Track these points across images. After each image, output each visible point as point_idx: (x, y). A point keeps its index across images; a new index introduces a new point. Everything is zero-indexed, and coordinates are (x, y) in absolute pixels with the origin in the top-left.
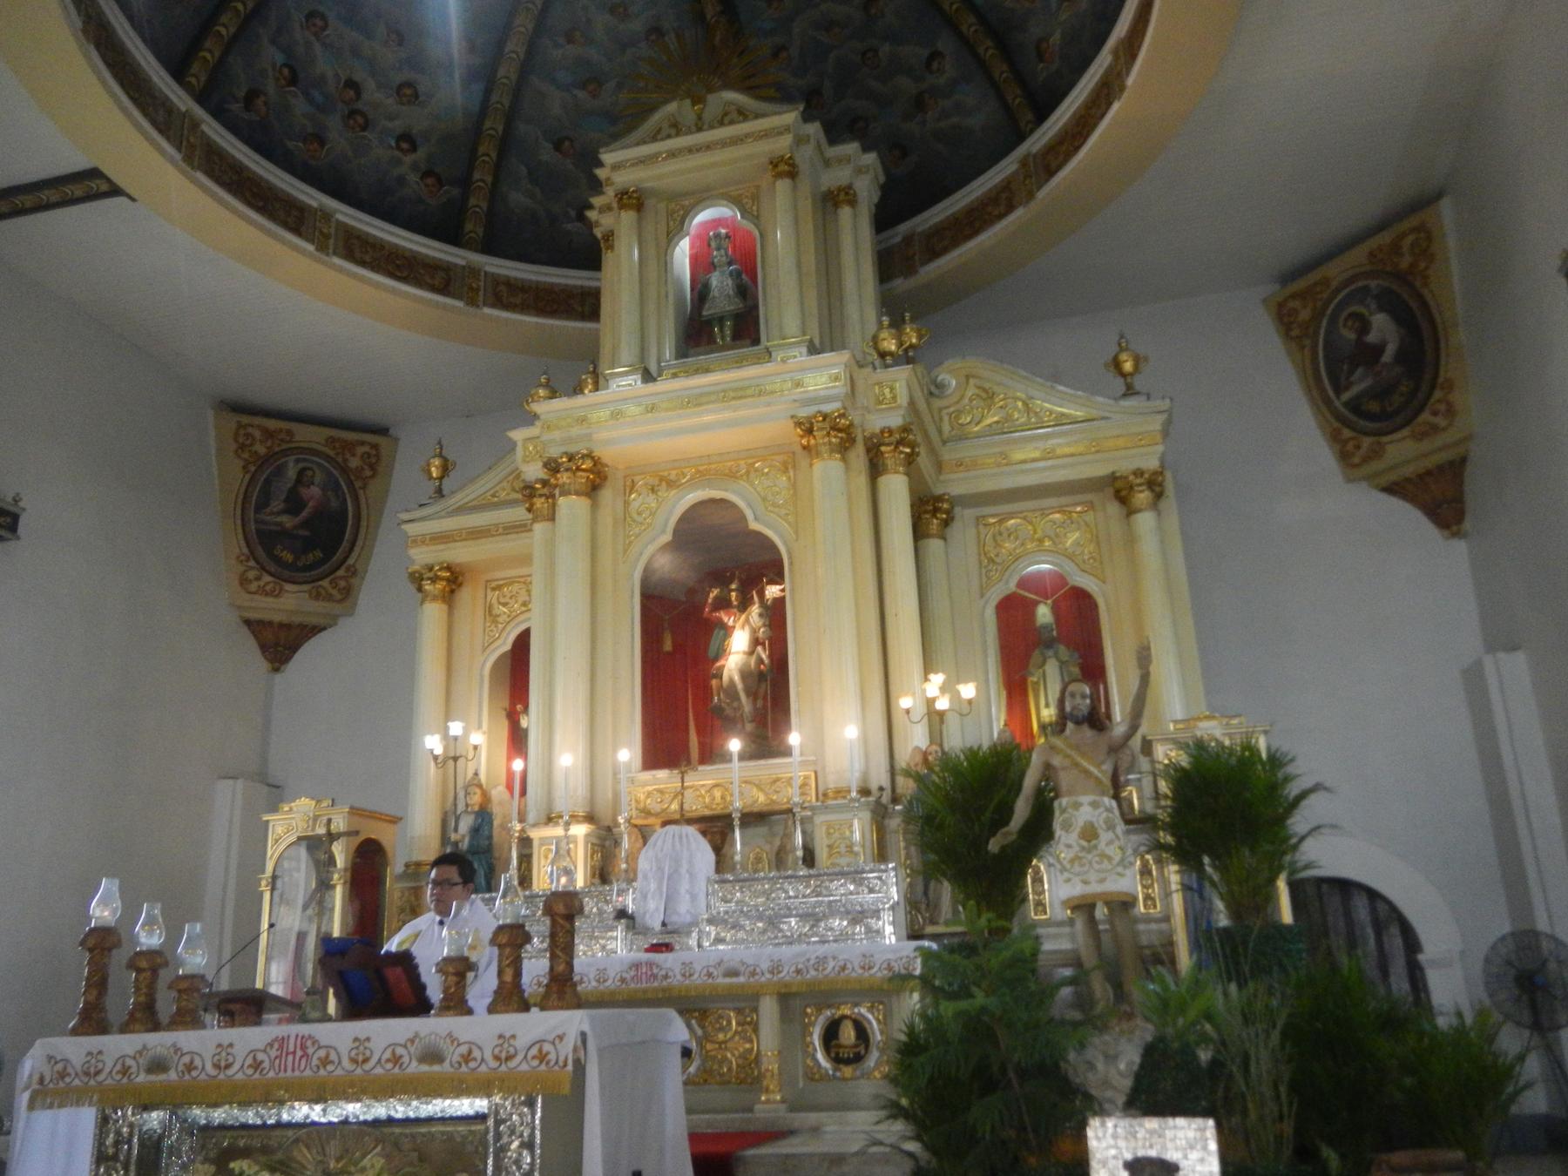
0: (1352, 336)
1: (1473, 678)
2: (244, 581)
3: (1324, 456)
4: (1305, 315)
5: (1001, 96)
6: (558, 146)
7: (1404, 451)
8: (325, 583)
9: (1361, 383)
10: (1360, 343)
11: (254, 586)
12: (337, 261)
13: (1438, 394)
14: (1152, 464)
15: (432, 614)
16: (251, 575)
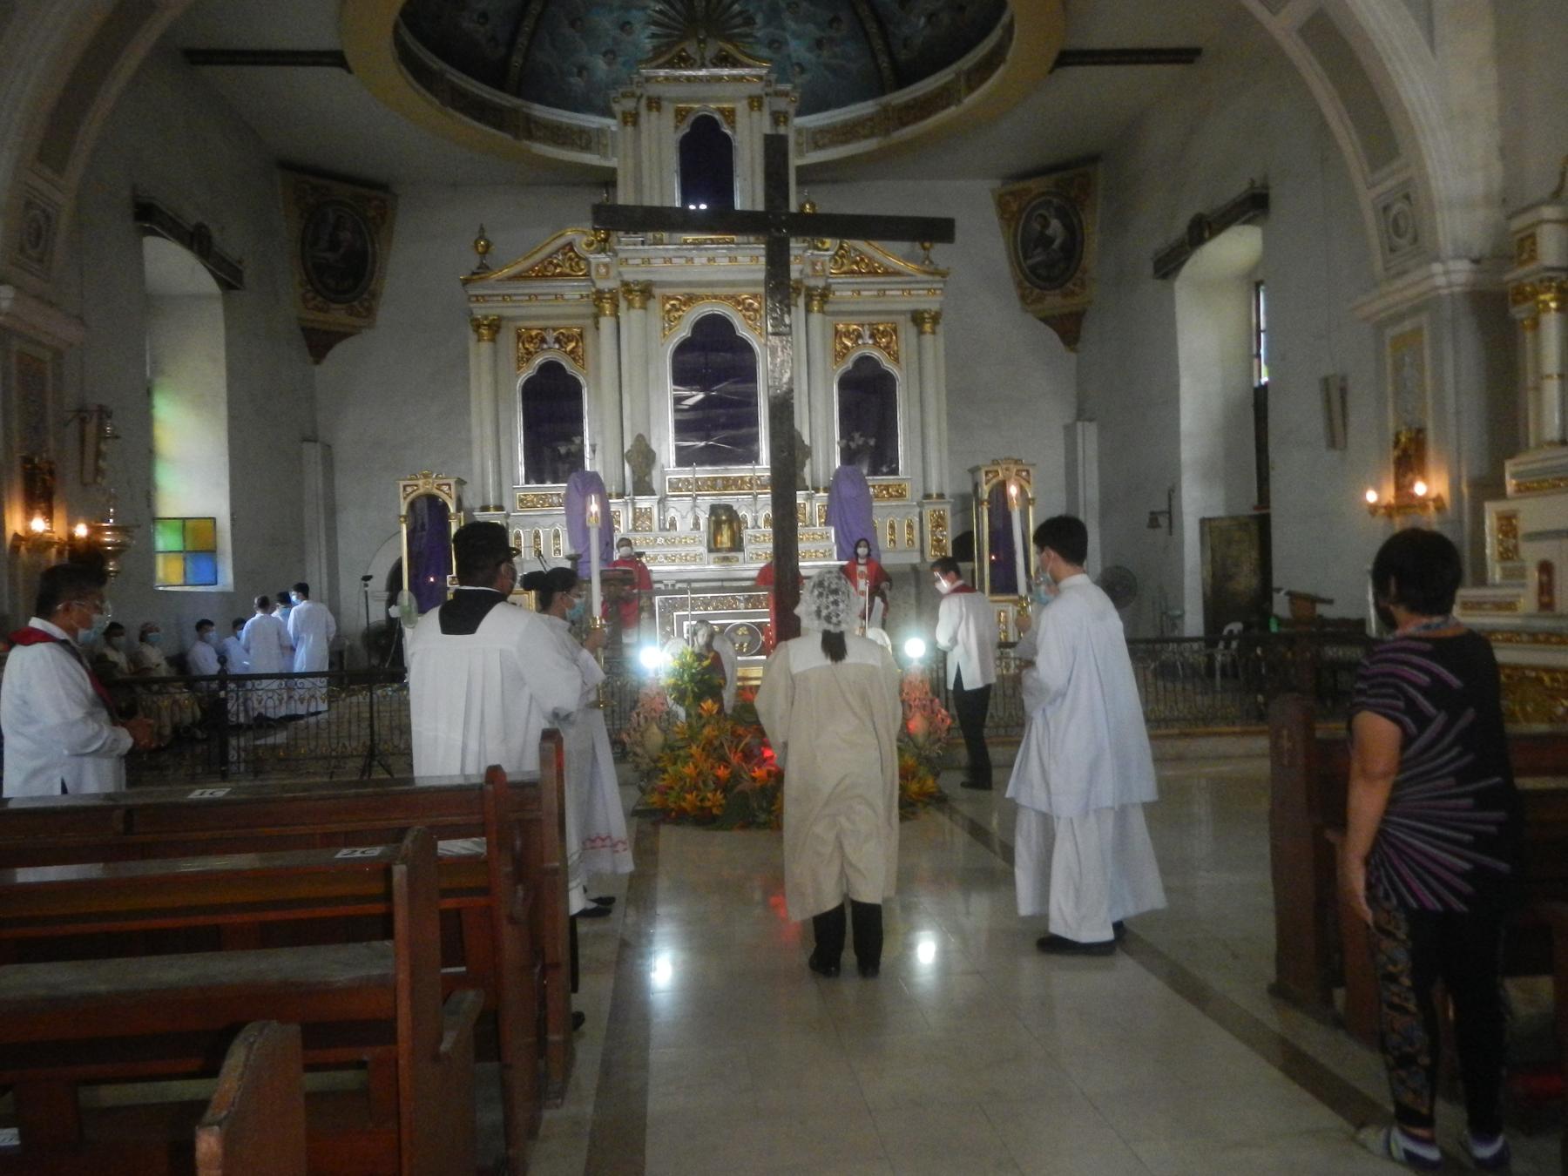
0: (1037, 227)
1: (1069, 431)
2: (305, 300)
3: (1014, 294)
4: (1014, 207)
5: (874, 57)
6: (573, 24)
7: (1054, 302)
8: (355, 303)
9: (1038, 257)
10: (1042, 233)
11: (310, 305)
12: (450, 110)
13: (1079, 274)
14: (935, 307)
15: (485, 347)
16: (310, 295)
